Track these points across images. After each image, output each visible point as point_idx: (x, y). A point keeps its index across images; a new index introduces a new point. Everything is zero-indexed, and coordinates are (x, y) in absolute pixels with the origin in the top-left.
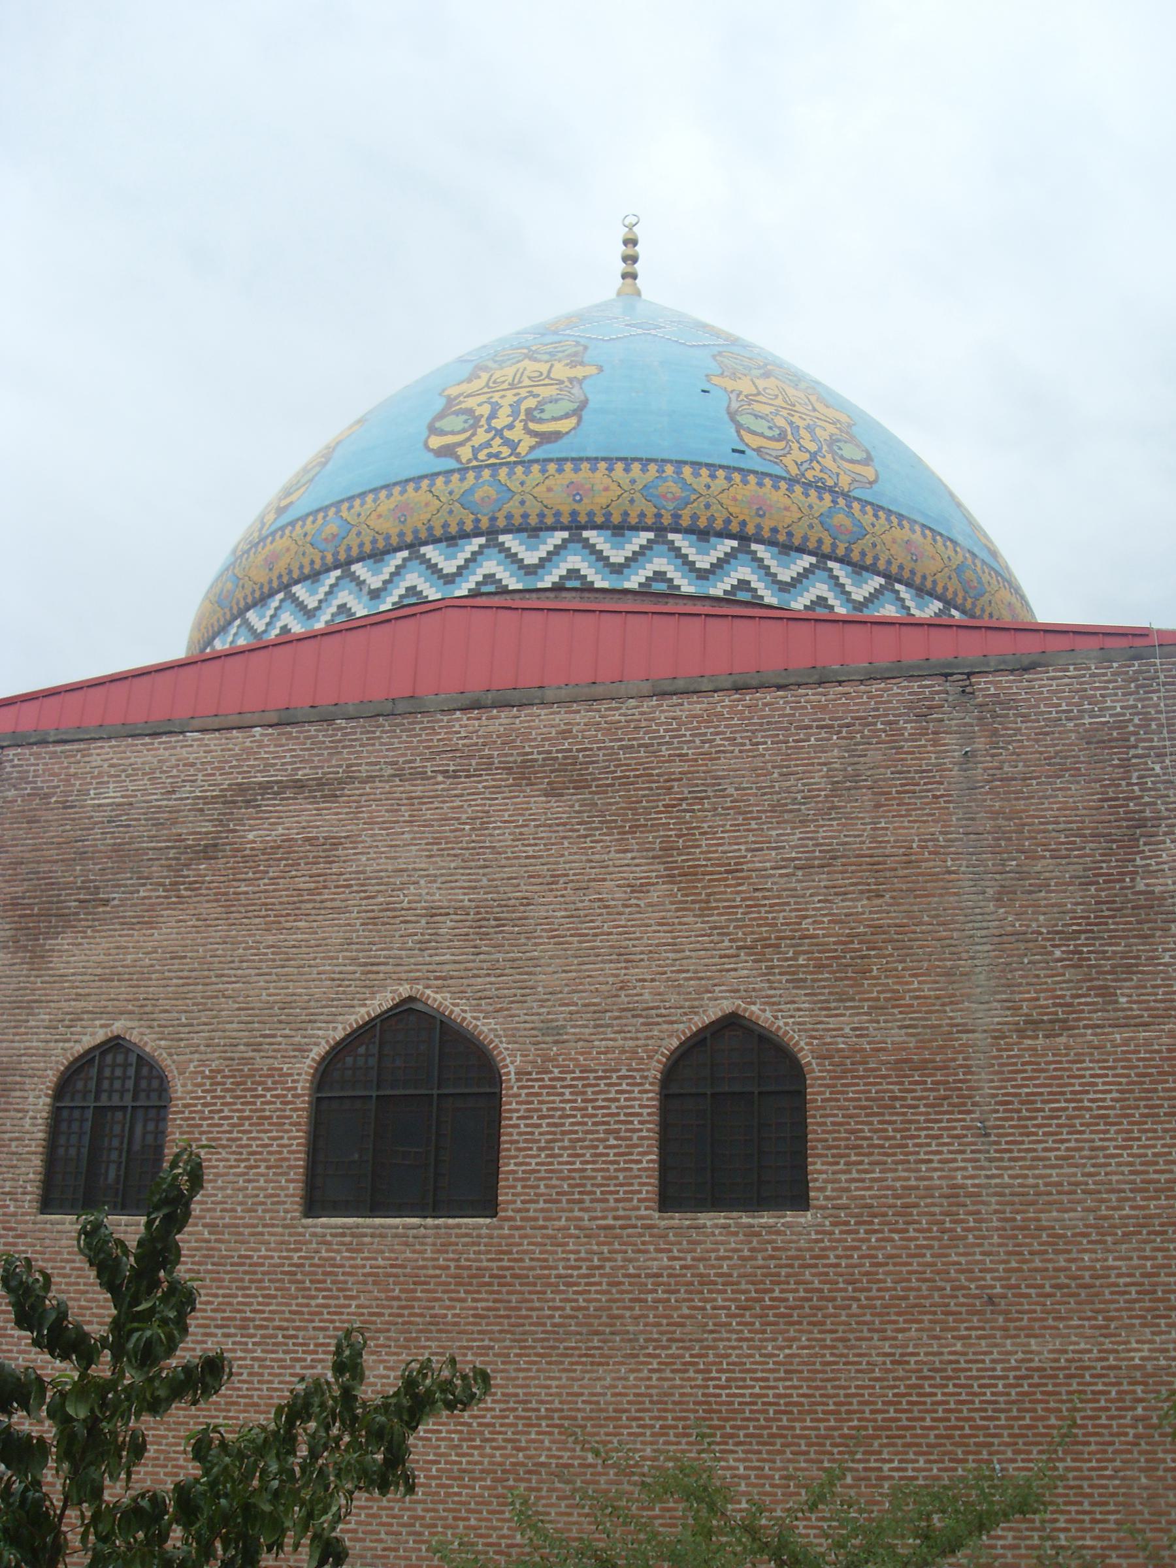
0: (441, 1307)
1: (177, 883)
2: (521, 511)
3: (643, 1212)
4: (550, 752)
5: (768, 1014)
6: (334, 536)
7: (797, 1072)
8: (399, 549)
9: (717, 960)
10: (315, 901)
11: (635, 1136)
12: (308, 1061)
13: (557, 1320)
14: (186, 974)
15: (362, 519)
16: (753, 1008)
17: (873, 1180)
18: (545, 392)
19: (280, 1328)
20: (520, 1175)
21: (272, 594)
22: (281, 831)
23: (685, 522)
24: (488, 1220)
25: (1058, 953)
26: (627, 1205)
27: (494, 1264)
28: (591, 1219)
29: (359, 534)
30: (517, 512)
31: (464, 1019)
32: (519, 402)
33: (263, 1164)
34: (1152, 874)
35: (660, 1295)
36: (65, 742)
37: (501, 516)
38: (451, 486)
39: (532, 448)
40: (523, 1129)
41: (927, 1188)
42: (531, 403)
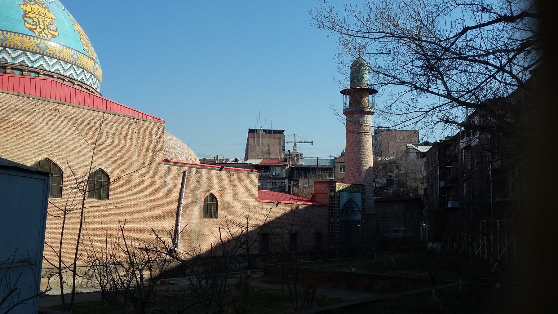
4: (72, 116)
5: (105, 169)
6: (2, 39)
8: (20, 50)
13: (71, 215)
18: (49, 21)
20: (66, 191)
22: (19, 119)
23: (76, 64)
24: (60, 199)
27: (61, 206)
28: (77, 199)
29: (10, 42)
30: (49, 52)
31: (57, 163)
32: (43, 21)
34: (156, 156)
37: (45, 52)
38: (34, 41)
39: (51, 38)
40: (67, 184)
42: (46, 23)
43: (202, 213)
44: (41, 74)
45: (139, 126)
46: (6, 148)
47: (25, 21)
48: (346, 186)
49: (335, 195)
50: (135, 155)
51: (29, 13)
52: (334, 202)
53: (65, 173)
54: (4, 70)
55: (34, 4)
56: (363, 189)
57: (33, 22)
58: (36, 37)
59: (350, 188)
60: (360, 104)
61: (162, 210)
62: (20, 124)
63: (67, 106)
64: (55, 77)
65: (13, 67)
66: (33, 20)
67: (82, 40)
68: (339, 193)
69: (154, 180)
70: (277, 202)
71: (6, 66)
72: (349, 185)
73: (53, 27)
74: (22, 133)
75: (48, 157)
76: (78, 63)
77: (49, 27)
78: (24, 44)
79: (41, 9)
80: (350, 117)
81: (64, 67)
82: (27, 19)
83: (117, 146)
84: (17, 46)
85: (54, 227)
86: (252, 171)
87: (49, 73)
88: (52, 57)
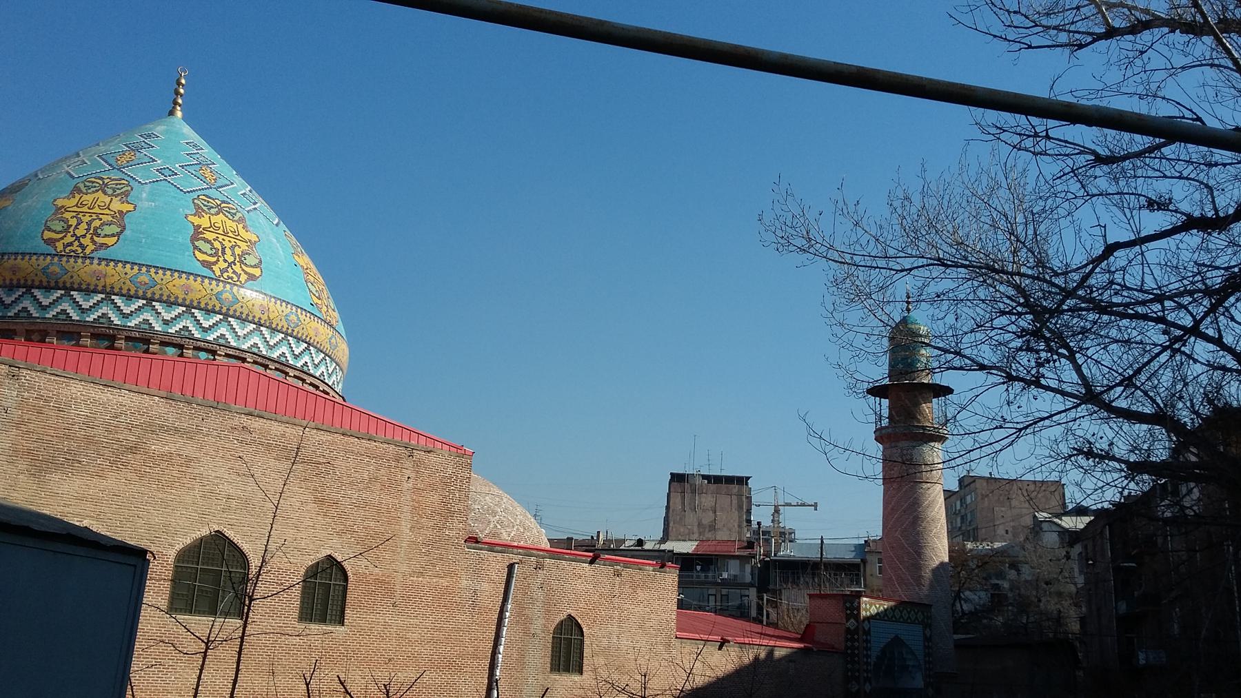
0: (219, 653)
1: (116, 461)
2: (241, 310)
3: (293, 622)
4: (277, 441)
7: (345, 577)
9: (327, 535)
10: (180, 482)
11: (293, 594)
12: (174, 550)
14: (120, 504)
15: (164, 282)
16: (336, 554)
17: (363, 618)
18: (244, 246)
19: (155, 659)
21: (95, 291)
23: (295, 334)
25: (423, 551)
26: (288, 619)
29: (161, 289)
30: (239, 310)
32: (232, 248)
33: (152, 591)
34: (450, 529)
35: (295, 652)
36: (57, 375)
37: (232, 309)
39: (246, 281)
41: (378, 622)
42: (238, 251)
43: (549, 660)
44: (220, 355)
45: (417, 464)
46: (135, 509)
47: (196, 248)
48: (886, 607)
49: (857, 627)
50: (405, 527)
51: (205, 232)
52: (856, 644)
53: (253, 564)
54: (146, 347)
55: (217, 214)
56: (925, 614)
57: (211, 249)
58: (216, 280)
59: (894, 611)
60: (912, 418)
61: (458, 653)
62: (168, 458)
63: (269, 422)
64: (248, 360)
65: (164, 340)
66: (212, 245)
67: (309, 284)
68: (869, 622)
69: (444, 582)
70: (722, 639)
71: (149, 338)
72: (892, 603)
73: (250, 260)
74: (169, 477)
75: (221, 528)
76: (298, 332)
77: (243, 259)
78: (189, 294)
79: (229, 223)
80: (892, 447)
81: (268, 340)
82: (200, 244)
83: (368, 507)
84: (175, 298)
85: (221, 684)
86: (663, 566)
87: (237, 353)
88: (243, 320)
